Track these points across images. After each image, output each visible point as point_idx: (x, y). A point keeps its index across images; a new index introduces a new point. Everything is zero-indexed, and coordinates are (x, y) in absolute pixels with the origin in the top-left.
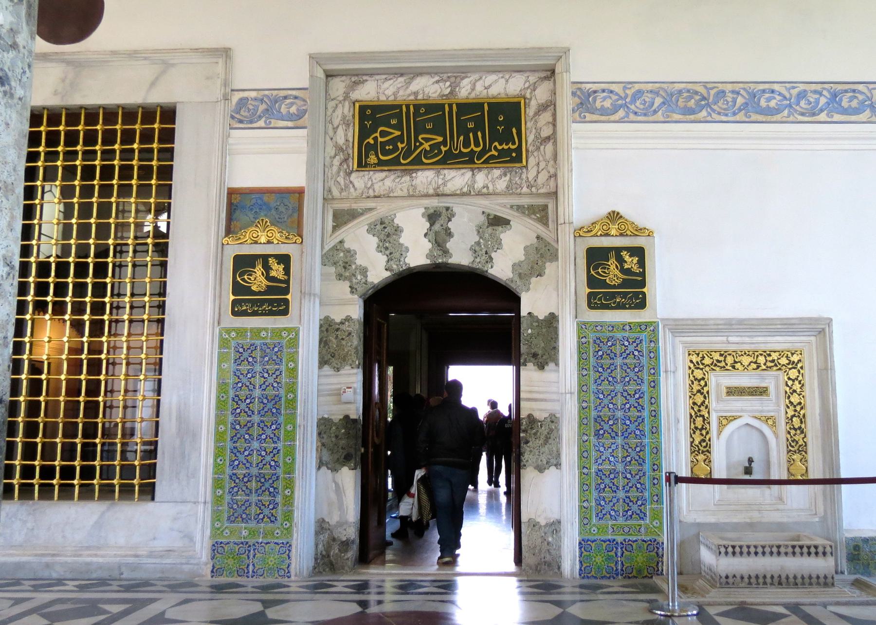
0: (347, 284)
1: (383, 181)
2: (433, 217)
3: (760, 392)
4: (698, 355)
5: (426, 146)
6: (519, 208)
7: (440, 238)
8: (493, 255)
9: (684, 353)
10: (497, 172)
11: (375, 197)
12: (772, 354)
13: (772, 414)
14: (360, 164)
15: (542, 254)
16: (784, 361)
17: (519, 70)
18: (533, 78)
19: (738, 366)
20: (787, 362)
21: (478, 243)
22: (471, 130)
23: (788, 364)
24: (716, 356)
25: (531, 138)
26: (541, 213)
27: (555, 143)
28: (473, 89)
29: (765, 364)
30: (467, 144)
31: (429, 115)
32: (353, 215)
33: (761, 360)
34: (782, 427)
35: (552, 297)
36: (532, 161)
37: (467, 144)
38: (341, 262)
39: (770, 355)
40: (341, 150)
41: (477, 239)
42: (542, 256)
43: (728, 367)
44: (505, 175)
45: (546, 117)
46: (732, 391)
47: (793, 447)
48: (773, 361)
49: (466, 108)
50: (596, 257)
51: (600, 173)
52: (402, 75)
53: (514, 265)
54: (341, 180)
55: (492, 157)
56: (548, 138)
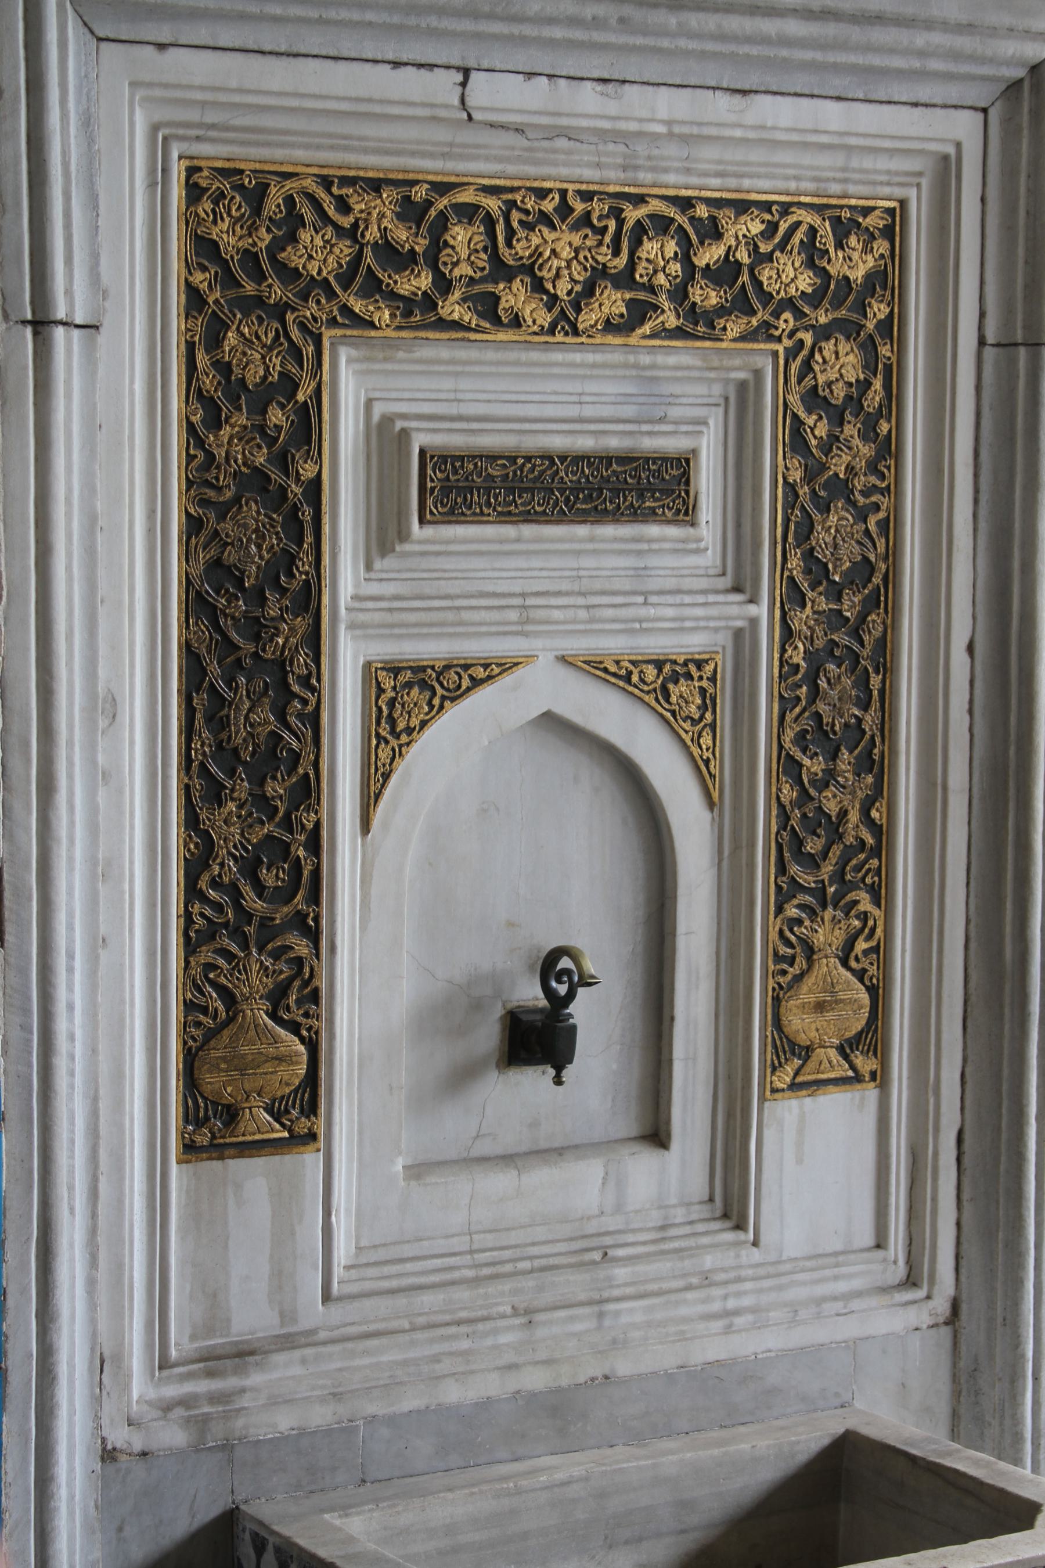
3: (638, 487)
4: (257, 197)
9: (158, 178)
12: (725, 216)
13: (694, 643)
20: (805, 282)
23: (815, 299)
24: (380, 217)
29: (680, 294)
39: (713, 232)
43: (453, 308)
46: (470, 486)
47: (813, 863)
48: (725, 273)
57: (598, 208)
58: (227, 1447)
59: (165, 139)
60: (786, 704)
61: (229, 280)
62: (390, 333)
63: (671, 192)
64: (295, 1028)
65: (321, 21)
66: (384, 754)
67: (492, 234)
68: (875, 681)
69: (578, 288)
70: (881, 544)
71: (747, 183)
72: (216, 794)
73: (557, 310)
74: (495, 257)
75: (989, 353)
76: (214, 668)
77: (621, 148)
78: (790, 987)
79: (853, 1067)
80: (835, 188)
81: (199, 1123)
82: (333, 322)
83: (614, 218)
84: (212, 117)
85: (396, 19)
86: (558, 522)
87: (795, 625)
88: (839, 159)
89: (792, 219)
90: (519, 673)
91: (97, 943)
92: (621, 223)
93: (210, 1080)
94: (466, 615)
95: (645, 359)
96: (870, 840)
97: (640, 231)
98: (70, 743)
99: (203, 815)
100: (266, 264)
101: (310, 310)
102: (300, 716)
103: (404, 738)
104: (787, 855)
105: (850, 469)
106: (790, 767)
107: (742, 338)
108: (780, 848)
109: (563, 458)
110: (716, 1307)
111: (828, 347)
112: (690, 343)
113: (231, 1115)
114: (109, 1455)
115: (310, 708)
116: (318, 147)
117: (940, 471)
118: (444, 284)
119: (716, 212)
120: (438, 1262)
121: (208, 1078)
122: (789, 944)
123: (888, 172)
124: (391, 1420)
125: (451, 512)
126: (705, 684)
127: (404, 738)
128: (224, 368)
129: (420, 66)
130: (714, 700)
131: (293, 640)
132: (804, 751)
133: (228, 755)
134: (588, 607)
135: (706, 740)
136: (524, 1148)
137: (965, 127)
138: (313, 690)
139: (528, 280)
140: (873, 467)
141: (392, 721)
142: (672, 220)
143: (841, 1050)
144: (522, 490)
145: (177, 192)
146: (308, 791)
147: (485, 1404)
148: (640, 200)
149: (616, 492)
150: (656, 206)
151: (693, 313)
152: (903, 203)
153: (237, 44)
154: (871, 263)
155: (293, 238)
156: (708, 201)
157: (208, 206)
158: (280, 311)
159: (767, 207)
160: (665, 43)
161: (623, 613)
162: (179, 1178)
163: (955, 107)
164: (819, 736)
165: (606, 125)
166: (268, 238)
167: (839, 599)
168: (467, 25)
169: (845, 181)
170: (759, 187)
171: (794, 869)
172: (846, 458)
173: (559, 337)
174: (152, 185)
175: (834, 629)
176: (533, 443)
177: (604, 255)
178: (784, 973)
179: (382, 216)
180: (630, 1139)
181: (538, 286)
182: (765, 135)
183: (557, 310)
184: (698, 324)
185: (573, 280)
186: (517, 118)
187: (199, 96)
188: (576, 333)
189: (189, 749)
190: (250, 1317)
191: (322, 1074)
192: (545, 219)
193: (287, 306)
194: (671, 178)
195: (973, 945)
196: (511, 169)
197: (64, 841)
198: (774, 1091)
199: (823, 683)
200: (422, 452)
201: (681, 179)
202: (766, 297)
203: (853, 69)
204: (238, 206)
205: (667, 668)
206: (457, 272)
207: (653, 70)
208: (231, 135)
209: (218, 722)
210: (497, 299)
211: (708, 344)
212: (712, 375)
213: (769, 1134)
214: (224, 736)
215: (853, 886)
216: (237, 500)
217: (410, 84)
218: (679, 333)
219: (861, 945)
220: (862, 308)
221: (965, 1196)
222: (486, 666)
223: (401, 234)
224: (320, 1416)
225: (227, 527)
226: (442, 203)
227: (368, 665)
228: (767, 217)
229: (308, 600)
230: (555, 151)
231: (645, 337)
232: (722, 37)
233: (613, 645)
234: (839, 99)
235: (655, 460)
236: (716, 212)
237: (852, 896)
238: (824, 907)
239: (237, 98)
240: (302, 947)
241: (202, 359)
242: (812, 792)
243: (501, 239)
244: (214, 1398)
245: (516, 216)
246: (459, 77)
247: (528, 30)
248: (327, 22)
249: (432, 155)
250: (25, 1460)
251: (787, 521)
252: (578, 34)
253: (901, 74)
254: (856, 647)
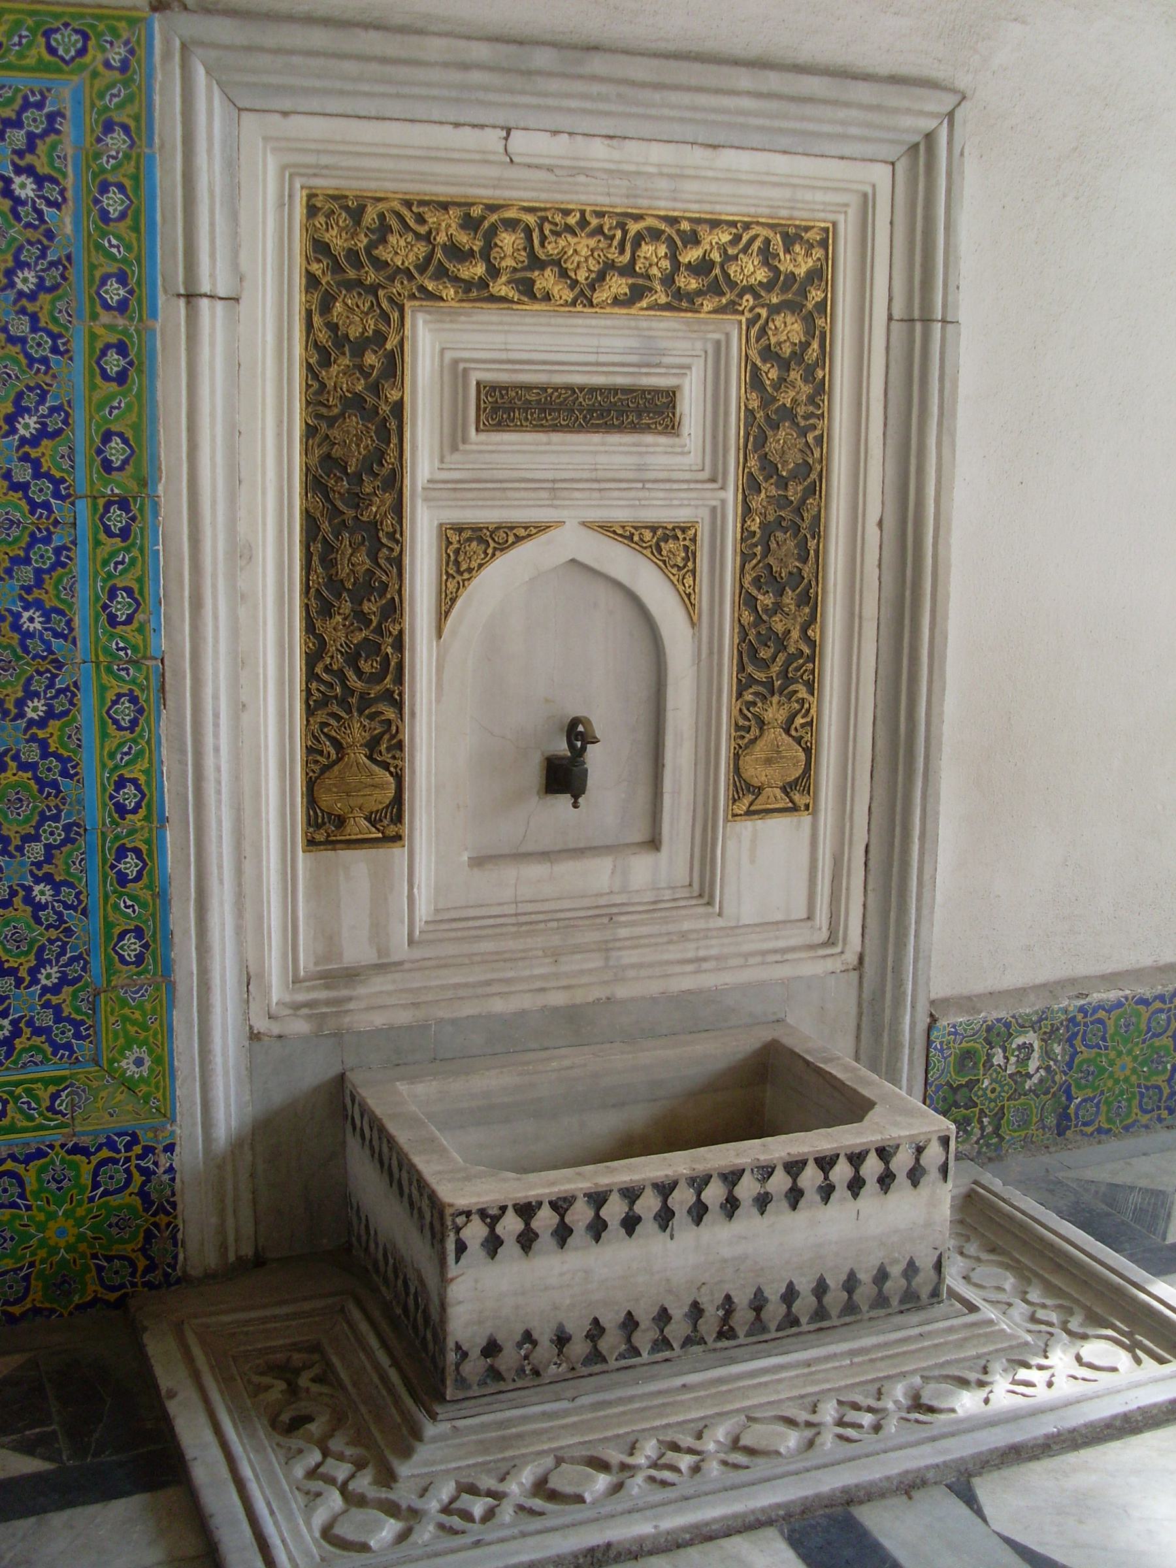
3: (642, 409)
9: (284, 202)
12: (703, 230)
13: (681, 515)
16: (751, 270)
19: (546, 280)
20: (762, 275)
23: (769, 286)
24: (448, 227)
29: (668, 280)
34: (722, 570)
39: (693, 239)
47: (765, 665)
48: (703, 267)
57: (607, 222)
58: (337, 1035)
59: (291, 176)
60: (745, 558)
61: (337, 268)
62: (453, 304)
63: (662, 213)
64: (385, 766)
65: (398, 96)
66: (452, 585)
67: (529, 238)
68: (812, 544)
69: (593, 275)
70: (817, 455)
71: (718, 208)
72: (327, 610)
73: (577, 290)
74: (532, 255)
75: (894, 325)
76: (325, 526)
77: (626, 183)
78: (747, 747)
79: (792, 801)
80: (784, 213)
81: (318, 827)
82: (413, 297)
83: (621, 231)
84: (325, 160)
85: (454, 94)
86: (579, 432)
87: (754, 505)
88: (787, 193)
89: (752, 233)
90: (551, 533)
91: (239, 707)
92: (625, 233)
93: (326, 800)
94: (510, 494)
95: (644, 324)
96: (807, 651)
97: (639, 239)
98: (214, 576)
99: (318, 624)
100: (364, 258)
101: (396, 288)
102: (388, 559)
103: (466, 576)
104: (745, 659)
105: (794, 401)
106: (749, 601)
107: (715, 311)
108: (740, 654)
109: (581, 389)
110: (691, 955)
111: (779, 320)
112: (676, 314)
113: (341, 822)
114: (255, 1037)
115: (395, 554)
116: (402, 181)
117: (859, 404)
118: (494, 272)
119: (695, 227)
120: (491, 922)
121: (324, 797)
122: (747, 719)
123: (824, 203)
124: (454, 1022)
125: (499, 424)
126: (687, 543)
127: (466, 576)
128: (333, 327)
129: (474, 126)
130: (694, 554)
131: (383, 509)
132: (759, 589)
133: (335, 585)
134: (600, 490)
135: (689, 581)
136: (558, 848)
137: (880, 175)
138: (397, 542)
139: (556, 269)
140: (811, 400)
141: (457, 563)
142: (663, 232)
143: (783, 789)
144: (552, 411)
145: (299, 211)
146: (394, 609)
147: (523, 1013)
148: (639, 218)
149: (621, 413)
150: (650, 222)
151: (679, 294)
152: (834, 224)
153: (341, 111)
154: (810, 263)
155: (383, 240)
156: (690, 220)
157: (322, 220)
158: (373, 290)
159: (733, 224)
160: (653, 112)
161: (632, 494)
162: (304, 860)
163: (871, 160)
164: (769, 580)
165: (612, 166)
166: (365, 241)
167: (786, 488)
168: (508, 98)
169: (792, 208)
170: (728, 211)
171: (750, 669)
172: (792, 394)
173: (579, 308)
174: (281, 205)
175: (781, 508)
176: (559, 379)
177: (613, 254)
178: (743, 737)
179: (449, 226)
180: (638, 844)
181: (564, 274)
182: (730, 175)
183: (577, 290)
184: (681, 301)
185: (589, 270)
186: (547, 161)
187: (313, 146)
188: (592, 305)
189: (308, 580)
190: (356, 950)
191: (406, 796)
192: (569, 229)
193: (380, 286)
194: (662, 204)
195: (878, 722)
196: (544, 196)
197: (210, 640)
198: (734, 815)
199: (773, 545)
200: (478, 384)
201: (670, 204)
202: (732, 285)
203: (794, 132)
204: (343, 218)
205: (659, 532)
206: (504, 264)
207: (648, 129)
208: (340, 173)
209: (328, 562)
210: (532, 282)
211: (689, 315)
212: (694, 335)
213: (731, 845)
214: (333, 571)
215: (794, 681)
216: (342, 414)
217: (467, 138)
218: (668, 307)
219: (799, 721)
220: (804, 293)
221: (870, 888)
222: (526, 528)
223: (463, 238)
224: (403, 1017)
225: (335, 433)
226: (494, 218)
227: (441, 525)
228: (734, 231)
229: (394, 482)
230: (576, 184)
231: (642, 309)
232: (695, 109)
233: (620, 514)
234: (785, 152)
235: (649, 392)
236: (695, 227)
237: (792, 688)
238: (773, 694)
239: (342, 148)
240: (390, 714)
241: (317, 320)
242: (765, 617)
243: (536, 242)
244: (328, 1002)
245: (547, 227)
246: (504, 134)
247: (550, 102)
248: (404, 96)
249: (485, 187)
250: (191, 1039)
251: (747, 435)
252: (588, 105)
253: (830, 136)
254: (798, 520)
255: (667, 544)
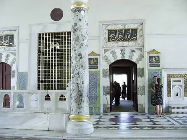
0: (107, 63)
1: (112, 44)
2: (122, 50)
5: (120, 37)
6: (137, 49)
7: (123, 55)
8: (133, 57)
10: (133, 42)
11: (111, 47)
14: (108, 41)
15: (142, 57)
17: (136, 23)
18: (139, 25)
21: (130, 55)
22: (128, 34)
24: (172, 75)
25: (139, 36)
26: (141, 50)
27: (143, 37)
28: (128, 27)
30: (127, 37)
31: (120, 31)
32: (108, 50)
33: (180, 76)
34: (183, 87)
35: (143, 64)
36: (139, 40)
37: (127, 37)
38: (106, 59)
40: (105, 38)
41: (130, 54)
42: (141, 57)
44: (134, 42)
45: (141, 32)
46: (174, 81)
49: (127, 30)
50: (151, 58)
51: (151, 42)
52: (115, 24)
53: (136, 59)
54: (105, 44)
55: (132, 39)
56: (142, 36)
184: (181, 77)
190: (169, 101)
255: (181, 86)
